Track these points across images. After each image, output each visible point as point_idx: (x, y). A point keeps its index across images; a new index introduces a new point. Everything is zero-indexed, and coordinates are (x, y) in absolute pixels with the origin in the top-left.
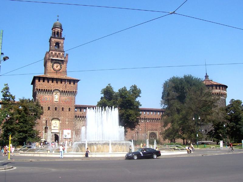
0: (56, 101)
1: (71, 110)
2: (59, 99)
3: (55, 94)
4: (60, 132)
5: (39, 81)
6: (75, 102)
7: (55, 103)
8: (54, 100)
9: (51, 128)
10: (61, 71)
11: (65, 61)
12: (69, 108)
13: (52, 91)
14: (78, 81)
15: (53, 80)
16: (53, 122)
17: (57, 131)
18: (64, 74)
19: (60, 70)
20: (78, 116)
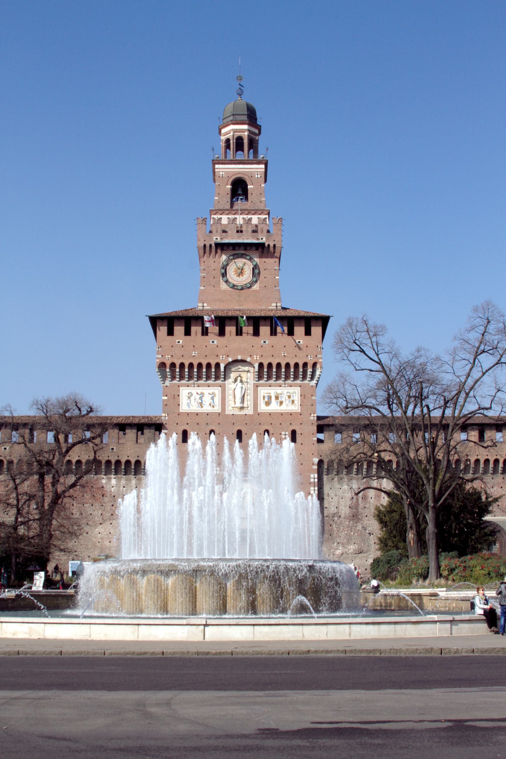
0: (239, 405)
3: (236, 380)
5: (170, 333)
10: (256, 287)
11: (271, 249)
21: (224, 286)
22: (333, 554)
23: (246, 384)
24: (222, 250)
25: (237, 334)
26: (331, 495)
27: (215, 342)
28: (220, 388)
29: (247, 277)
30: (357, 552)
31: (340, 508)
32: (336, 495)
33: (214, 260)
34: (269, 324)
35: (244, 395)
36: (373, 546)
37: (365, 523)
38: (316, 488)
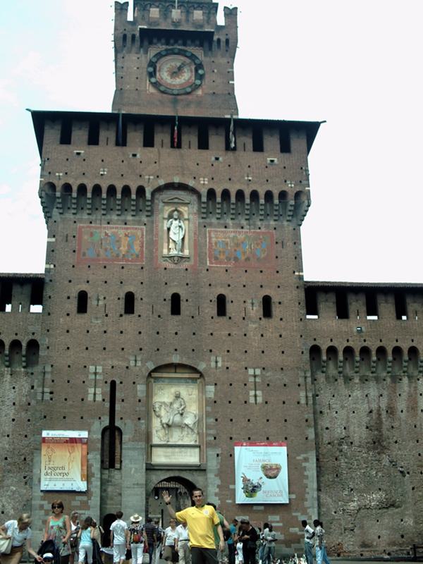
0: (174, 252)
1: (276, 310)
2: (197, 246)
4: (213, 464)
5: (66, 139)
6: (298, 257)
7: (170, 265)
8: (165, 251)
9: (148, 436)
10: (200, 92)
11: (223, 44)
12: (267, 303)
13: (148, 195)
14: (309, 130)
15: (149, 126)
16: (164, 395)
17: (192, 458)
18: (220, 108)
19: (197, 87)
20: (332, 351)
21: (152, 90)
22: (344, 510)
23: (187, 222)
24: (151, 43)
25: (172, 146)
26: (334, 406)
27: (138, 156)
28: (144, 227)
29: (187, 76)
30: (384, 505)
31: (352, 428)
32: (343, 407)
33: (139, 56)
34: (224, 134)
35: (183, 239)
36: (410, 495)
37: (394, 453)
38: (310, 395)
